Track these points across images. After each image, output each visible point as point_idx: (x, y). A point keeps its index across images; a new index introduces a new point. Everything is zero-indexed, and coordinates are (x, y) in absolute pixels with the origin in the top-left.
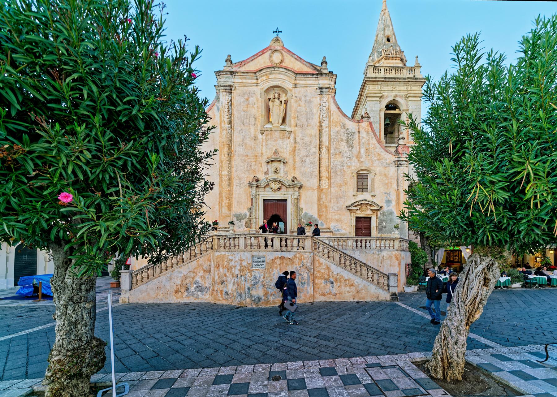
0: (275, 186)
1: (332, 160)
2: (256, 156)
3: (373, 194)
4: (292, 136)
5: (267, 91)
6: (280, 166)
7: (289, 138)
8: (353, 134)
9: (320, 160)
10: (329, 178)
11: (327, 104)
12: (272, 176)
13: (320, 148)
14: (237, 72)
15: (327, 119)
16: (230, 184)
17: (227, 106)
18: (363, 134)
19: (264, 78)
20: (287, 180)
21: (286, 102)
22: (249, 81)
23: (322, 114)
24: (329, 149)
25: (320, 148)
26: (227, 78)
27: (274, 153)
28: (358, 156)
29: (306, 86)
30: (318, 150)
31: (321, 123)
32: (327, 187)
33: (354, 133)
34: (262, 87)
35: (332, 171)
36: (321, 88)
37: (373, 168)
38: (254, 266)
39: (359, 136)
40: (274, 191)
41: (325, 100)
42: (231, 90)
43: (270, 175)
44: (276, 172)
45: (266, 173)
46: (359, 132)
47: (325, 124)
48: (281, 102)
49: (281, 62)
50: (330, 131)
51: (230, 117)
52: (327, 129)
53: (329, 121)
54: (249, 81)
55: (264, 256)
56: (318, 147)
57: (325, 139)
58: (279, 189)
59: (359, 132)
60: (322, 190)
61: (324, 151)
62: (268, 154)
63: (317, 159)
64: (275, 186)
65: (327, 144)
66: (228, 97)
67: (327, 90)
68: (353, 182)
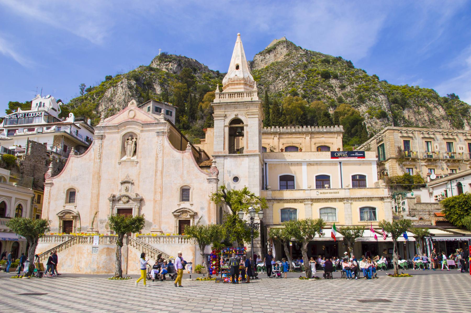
0: (125, 199)
1: (164, 179)
2: (115, 179)
3: (191, 203)
4: (138, 165)
6: (129, 185)
7: (136, 166)
8: (179, 161)
9: (156, 180)
10: (161, 193)
11: (162, 142)
12: (124, 193)
13: (156, 172)
14: (106, 127)
15: (161, 152)
16: (98, 200)
17: (99, 148)
18: (186, 161)
20: (133, 196)
22: (114, 131)
23: (158, 149)
24: (162, 173)
25: (156, 172)
26: (100, 130)
28: (182, 176)
29: (149, 131)
30: (154, 174)
31: (157, 154)
32: (159, 199)
33: (179, 160)
35: (163, 188)
36: (158, 132)
37: (192, 185)
39: (183, 162)
40: (125, 203)
41: (161, 139)
42: (102, 137)
43: (122, 192)
44: (127, 190)
45: (120, 191)
46: (183, 159)
47: (160, 155)
49: (134, 116)
50: (163, 160)
51: (101, 155)
52: (161, 159)
53: (163, 153)
54: (114, 131)
56: (154, 171)
58: (128, 202)
59: (183, 159)
60: (156, 201)
61: (159, 174)
62: (123, 178)
63: (154, 180)
64: (125, 199)
66: (100, 141)
67: (162, 133)
68: (177, 194)
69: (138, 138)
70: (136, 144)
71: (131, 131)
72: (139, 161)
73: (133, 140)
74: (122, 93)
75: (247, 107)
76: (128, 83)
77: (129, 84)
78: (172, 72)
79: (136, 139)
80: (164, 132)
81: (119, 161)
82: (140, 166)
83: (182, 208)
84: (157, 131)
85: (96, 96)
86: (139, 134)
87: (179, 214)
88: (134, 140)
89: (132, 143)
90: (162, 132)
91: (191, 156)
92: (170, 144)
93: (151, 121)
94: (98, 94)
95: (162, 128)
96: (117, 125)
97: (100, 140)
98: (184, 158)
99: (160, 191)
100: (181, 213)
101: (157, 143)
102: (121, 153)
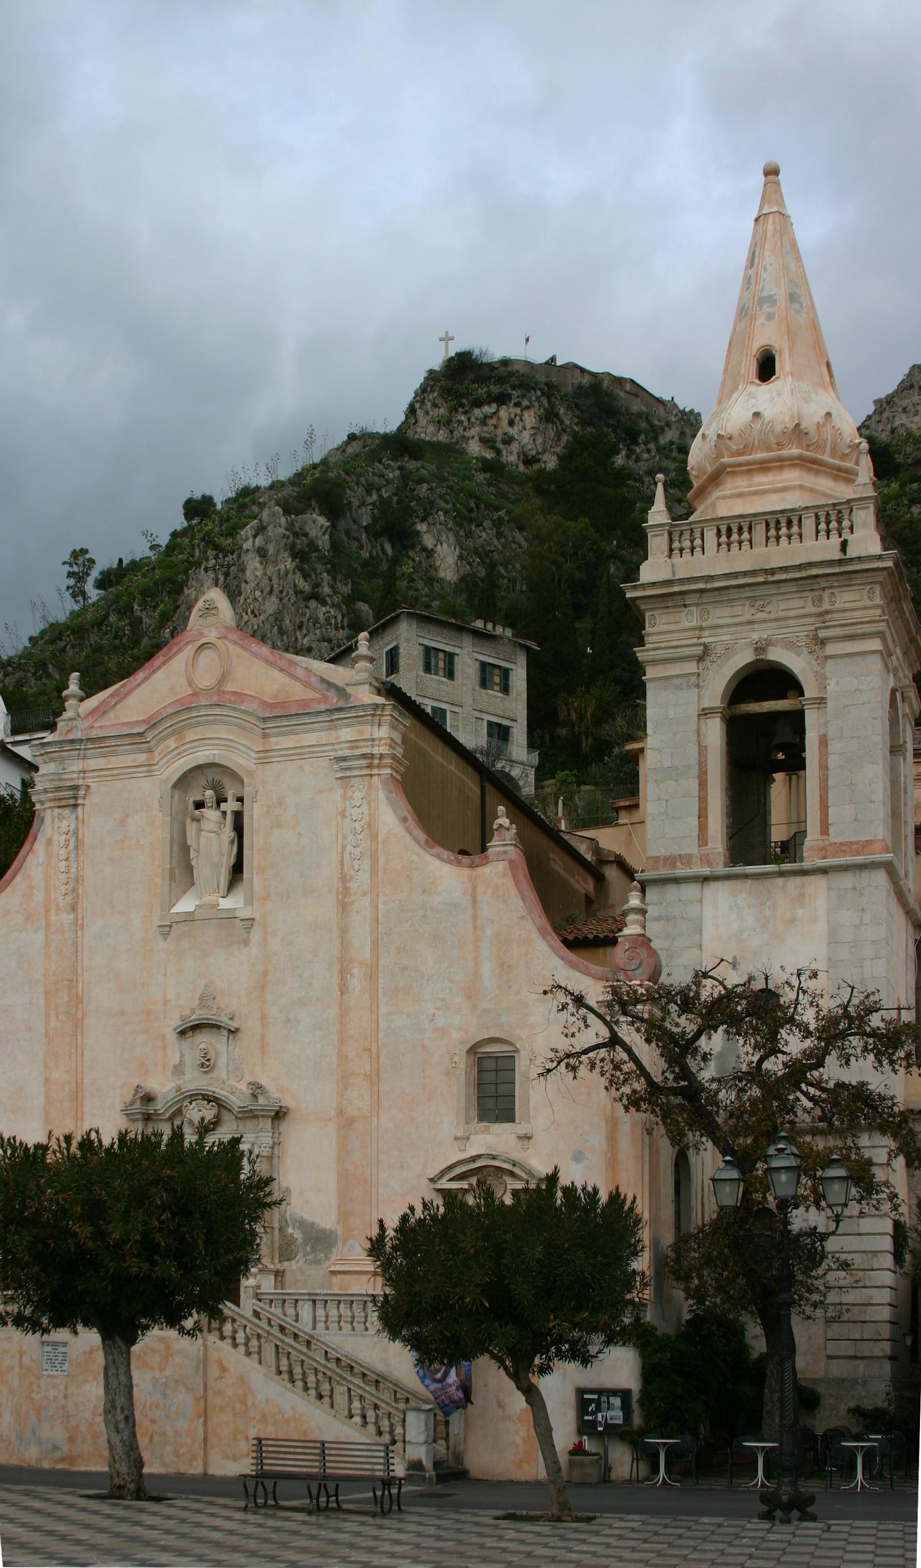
5: (183, 782)
11: (365, 809)
15: (367, 864)
19: (172, 743)
21: (238, 817)
27: (202, 998)
29: (300, 753)
31: (344, 878)
34: (164, 776)
36: (344, 759)
38: (45, 1366)
41: (358, 795)
48: (224, 813)
52: (366, 902)
53: (374, 871)
55: (65, 1344)
57: (360, 934)
65: (367, 955)
67: (363, 762)
69: (247, 792)
70: (238, 828)
71: (211, 760)
72: (257, 916)
73: (223, 806)
74: (265, 581)
75: (821, 600)
76: (290, 527)
77: (296, 535)
78: (513, 458)
79: (240, 800)
80: (372, 756)
81: (162, 917)
82: (265, 939)
83: (479, 1156)
84: (340, 754)
85: (144, 605)
86: (251, 774)
87: (464, 1185)
88: (230, 806)
89: (221, 824)
90: (364, 756)
91: (517, 883)
92: (405, 820)
93: (304, 703)
94: (148, 595)
95: (367, 731)
96: (141, 730)
97: (66, 812)
98: (481, 889)
99: (368, 1068)
100: (474, 1181)
101: (343, 816)
102: (172, 878)
